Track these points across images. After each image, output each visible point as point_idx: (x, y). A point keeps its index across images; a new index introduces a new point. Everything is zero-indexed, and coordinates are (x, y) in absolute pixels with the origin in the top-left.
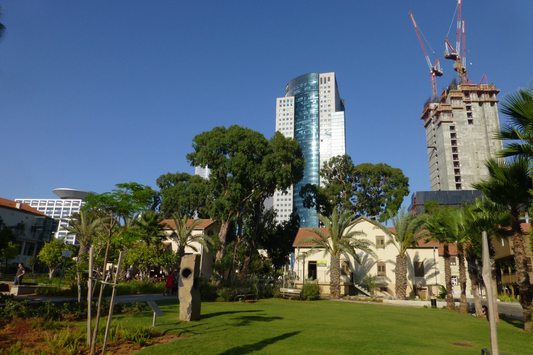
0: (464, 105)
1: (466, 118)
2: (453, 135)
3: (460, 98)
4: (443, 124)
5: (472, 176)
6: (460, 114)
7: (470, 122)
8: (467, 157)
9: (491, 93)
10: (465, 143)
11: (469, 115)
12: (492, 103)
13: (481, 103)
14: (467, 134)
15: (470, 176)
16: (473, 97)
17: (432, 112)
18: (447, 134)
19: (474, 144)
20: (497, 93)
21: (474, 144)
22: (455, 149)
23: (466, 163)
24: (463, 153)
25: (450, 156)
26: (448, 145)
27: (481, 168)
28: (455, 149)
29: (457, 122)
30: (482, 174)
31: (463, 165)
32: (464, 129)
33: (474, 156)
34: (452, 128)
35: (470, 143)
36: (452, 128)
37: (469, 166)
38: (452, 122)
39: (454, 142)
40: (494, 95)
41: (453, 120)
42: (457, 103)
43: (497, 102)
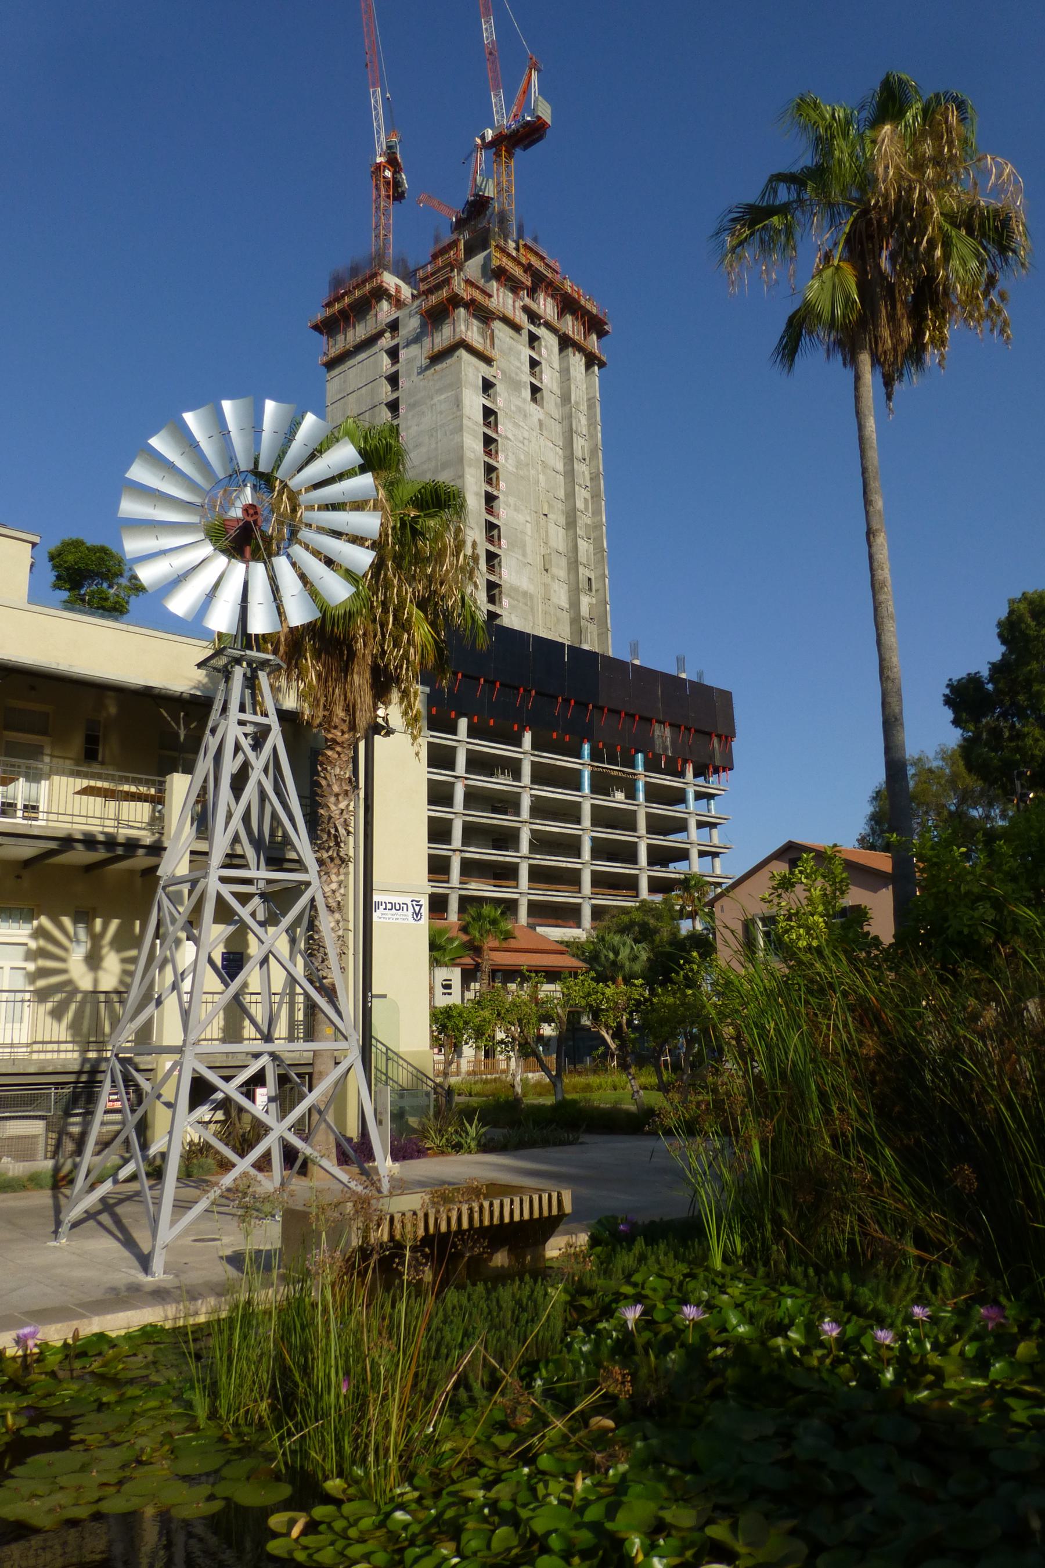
0: (522, 319)
1: (526, 378)
2: (489, 413)
3: (514, 287)
4: (463, 353)
5: (531, 597)
6: (511, 349)
7: (535, 390)
8: (521, 518)
9: (595, 325)
10: (519, 464)
11: (534, 364)
12: (591, 360)
13: (565, 343)
14: (526, 434)
15: (525, 594)
16: (546, 306)
17: (385, 305)
18: (473, 402)
19: (541, 477)
20: (602, 334)
21: (541, 477)
22: (490, 470)
23: (518, 544)
24: (512, 500)
25: (477, 494)
26: (474, 446)
27: (553, 577)
28: (490, 470)
29: (504, 372)
30: (555, 599)
31: (512, 545)
32: (519, 409)
33: (538, 523)
34: (487, 386)
35: (533, 472)
36: (487, 386)
37: (524, 555)
38: (488, 361)
39: (489, 441)
40: (594, 337)
41: (494, 354)
42: (502, 300)
43: (602, 365)
